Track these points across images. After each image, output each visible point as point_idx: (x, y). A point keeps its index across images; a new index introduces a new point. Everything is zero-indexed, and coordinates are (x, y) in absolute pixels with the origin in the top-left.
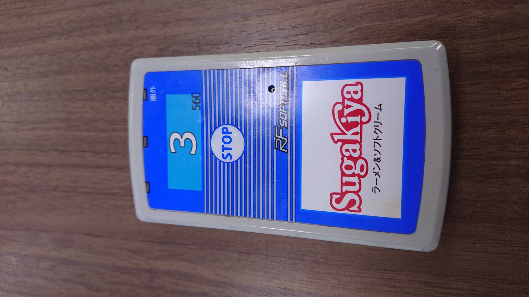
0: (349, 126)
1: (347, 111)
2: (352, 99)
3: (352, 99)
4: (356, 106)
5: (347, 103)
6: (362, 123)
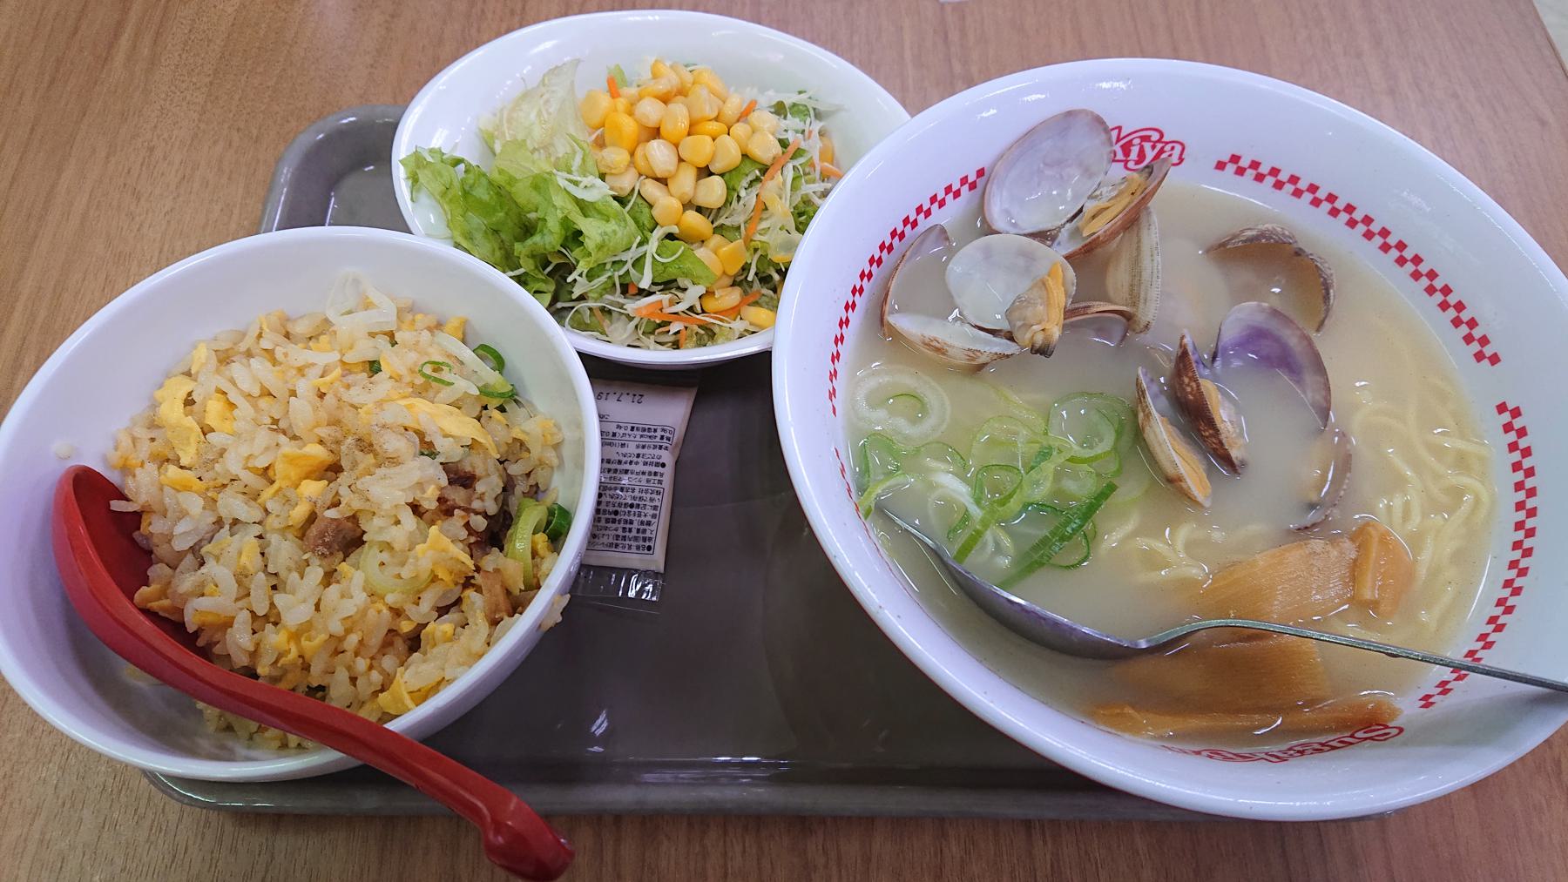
0: (1126, 149)
1: (1147, 146)
2: (1162, 151)
3: (1162, 151)
4: (1150, 154)
5: (1159, 146)
6: (1126, 162)
